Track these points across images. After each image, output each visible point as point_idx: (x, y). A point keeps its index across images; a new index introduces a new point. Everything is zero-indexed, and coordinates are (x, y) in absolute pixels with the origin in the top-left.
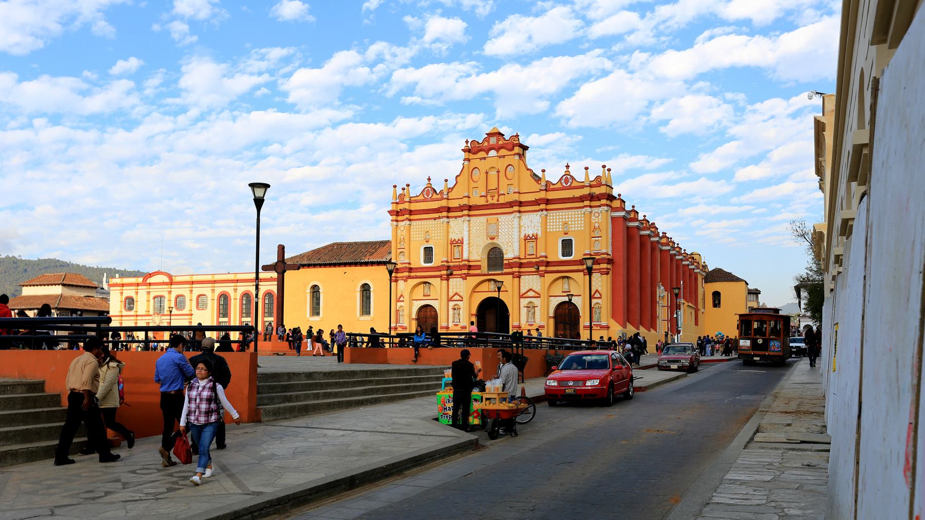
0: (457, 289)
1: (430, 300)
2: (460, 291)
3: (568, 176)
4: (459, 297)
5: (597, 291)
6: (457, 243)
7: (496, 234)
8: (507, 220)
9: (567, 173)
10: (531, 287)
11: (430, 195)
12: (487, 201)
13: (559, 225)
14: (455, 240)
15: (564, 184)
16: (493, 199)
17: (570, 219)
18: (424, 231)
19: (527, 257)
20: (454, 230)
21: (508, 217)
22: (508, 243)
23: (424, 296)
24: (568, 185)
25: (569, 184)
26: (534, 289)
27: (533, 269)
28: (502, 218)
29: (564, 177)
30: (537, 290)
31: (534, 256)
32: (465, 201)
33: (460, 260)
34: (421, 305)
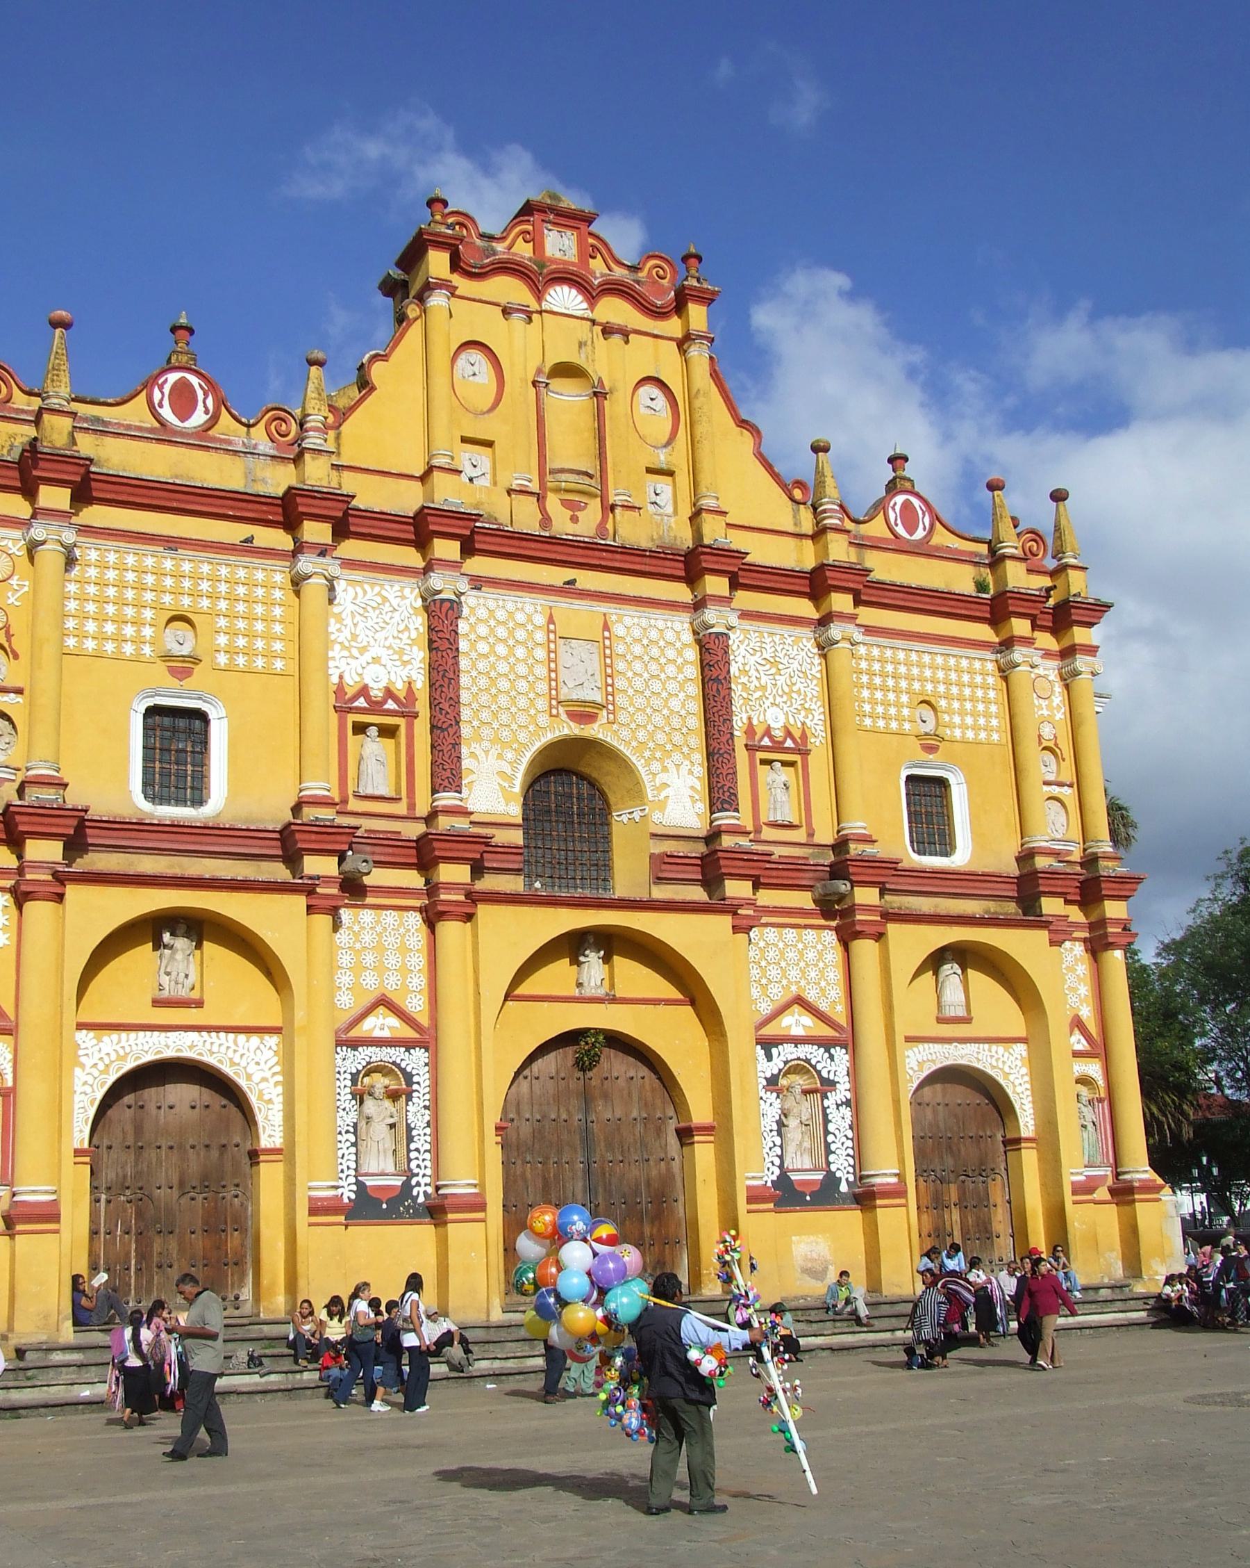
0: (381, 969)
1: (198, 1029)
2: (405, 989)
3: (916, 502)
4: (393, 1021)
5: (1078, 1024)
6: (375, 707)
7: (598, 697)
8: (654, 635)
9: (908, 485)
10: (794, 988)
11: (198, 418)
12: (546, 520)
13: (898, 705)
14: (364, 691)
15: (900, 530)
16: (574, 519)
17: (941, 688)
18: (157, 607)
19: (768, 834)
20: (354, 637)
21: (661, 624)
22: (668, 754)
23: (157, 1003)
24: (913, 538)
25: (920, 534)
26: (811, 996)
27: (804, 900)
28: (628, 621)
29: (900, 499)
30: (823, 1006)
31: (800, 836)
32: (447, 493)
33: (401, 808)
34: (129, 1065)
